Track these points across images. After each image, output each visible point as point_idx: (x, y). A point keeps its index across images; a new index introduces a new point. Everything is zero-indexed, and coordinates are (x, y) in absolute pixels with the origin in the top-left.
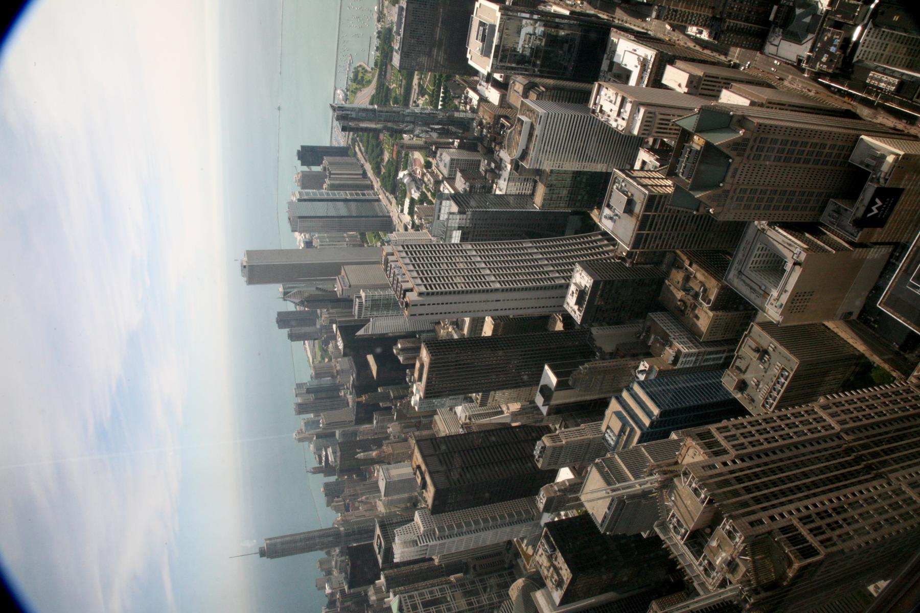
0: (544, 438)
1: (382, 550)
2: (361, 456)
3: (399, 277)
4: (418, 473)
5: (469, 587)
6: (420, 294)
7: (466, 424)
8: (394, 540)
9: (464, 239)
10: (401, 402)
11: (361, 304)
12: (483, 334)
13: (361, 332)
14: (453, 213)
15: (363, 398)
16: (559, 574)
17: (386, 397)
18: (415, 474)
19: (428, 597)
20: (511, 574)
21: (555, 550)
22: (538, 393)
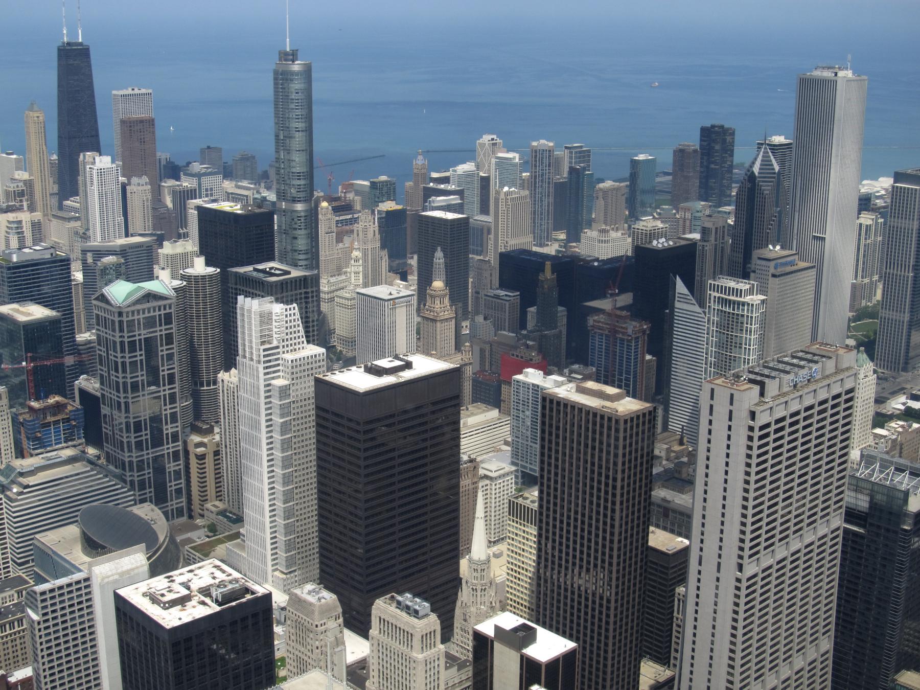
0: (433, 617)
1: (261, 275)
2: (439, 257)
3: (791, 377)
4: (397, 363)
5: (168, 429)
6: (753, 415)
7: (475, 468)
8: (277, 300)
9: (851, 515)
10: (532, 346)
11: (739, 293)
12: (651, 528)
13: (681, 287)
14: (906, 501)
15: (548, 274)
16: (173, 603)
17: (547, 320)
18: (397, 357)
19: (163, 351)
20: (180, 513)
21: (220, 604)
22: (522, 621)
